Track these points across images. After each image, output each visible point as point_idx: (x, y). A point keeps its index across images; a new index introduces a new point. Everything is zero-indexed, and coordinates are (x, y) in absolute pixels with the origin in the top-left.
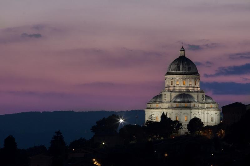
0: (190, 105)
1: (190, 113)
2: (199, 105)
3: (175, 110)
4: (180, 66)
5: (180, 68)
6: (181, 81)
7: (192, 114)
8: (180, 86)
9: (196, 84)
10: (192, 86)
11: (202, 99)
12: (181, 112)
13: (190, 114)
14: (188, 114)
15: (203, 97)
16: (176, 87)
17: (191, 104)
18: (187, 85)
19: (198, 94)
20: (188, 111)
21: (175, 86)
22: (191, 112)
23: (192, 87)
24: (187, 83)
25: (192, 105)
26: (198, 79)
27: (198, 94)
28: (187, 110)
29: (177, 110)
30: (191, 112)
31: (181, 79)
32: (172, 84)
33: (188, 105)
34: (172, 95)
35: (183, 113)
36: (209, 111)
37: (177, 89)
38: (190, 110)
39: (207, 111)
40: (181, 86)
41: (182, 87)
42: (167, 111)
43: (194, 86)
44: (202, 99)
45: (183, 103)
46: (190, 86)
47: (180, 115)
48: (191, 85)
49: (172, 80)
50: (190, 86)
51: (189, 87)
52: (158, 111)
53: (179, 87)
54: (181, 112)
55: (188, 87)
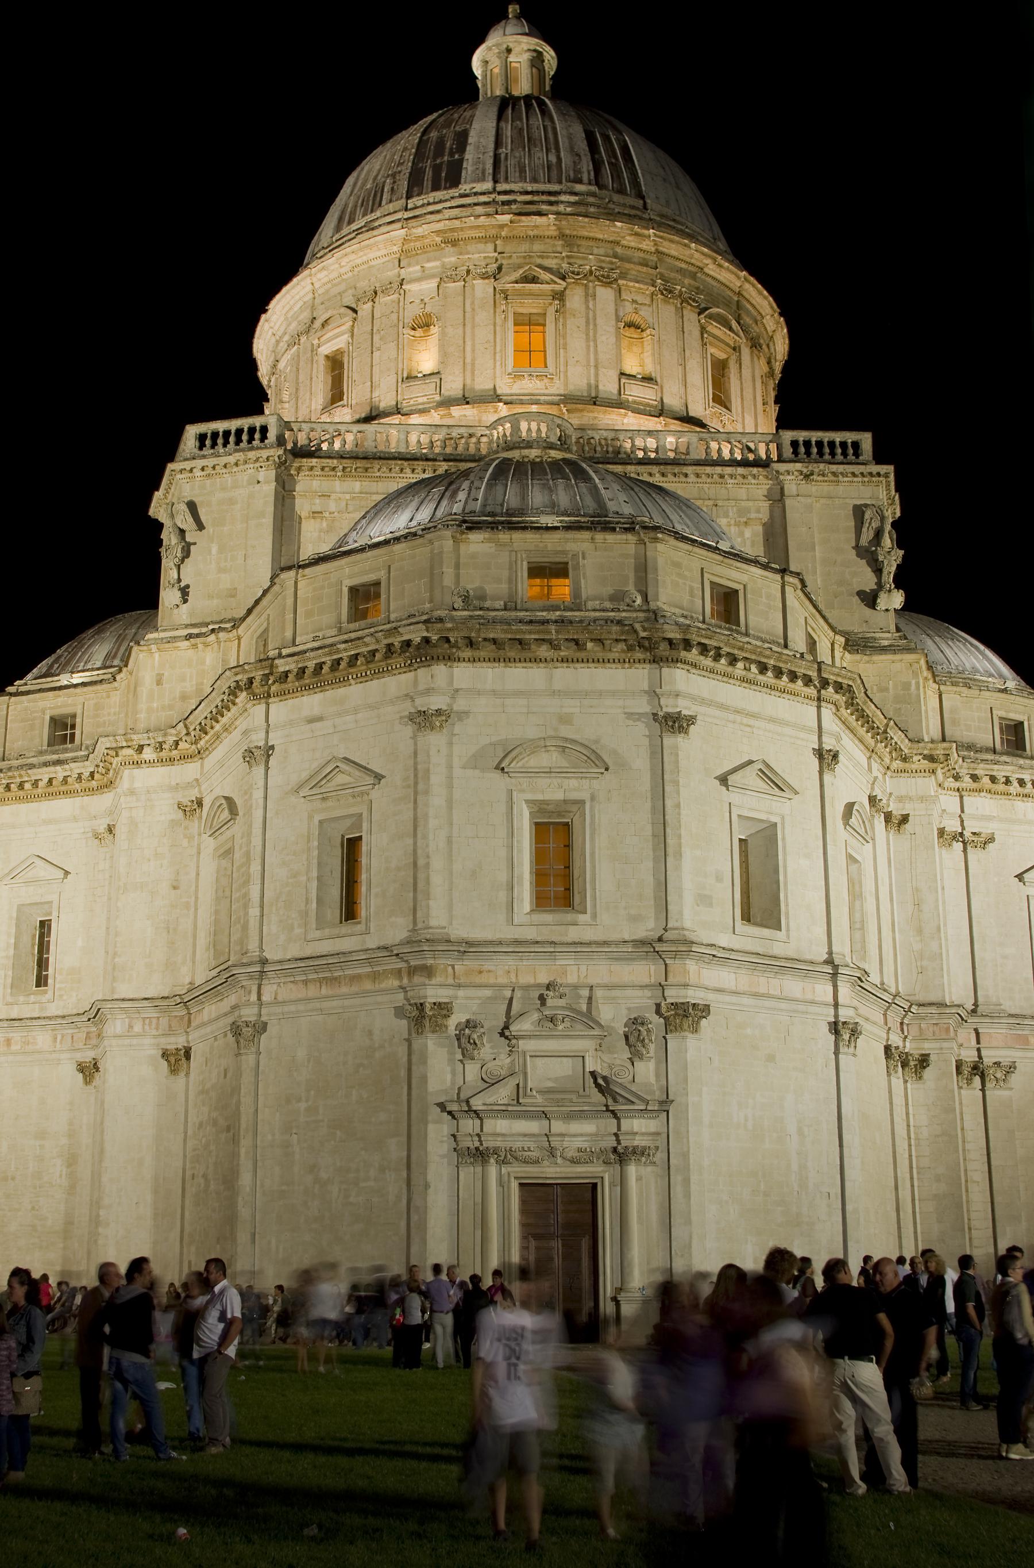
0: (643, 571)
1: (641, 730)
2: (812, 644)
3: (312, 702)
4: (462, 139)
5: (470, 155)
6: (483, 316)
7: (688, 750)
8: (453, 386)
9: (721, 399)
10: (673, 401)
11: (867, 580)
12: (424, 720)
13: (641, 762)
14: (594, 759)
15: (869, 555)
16: (398, 411)
17: (666, 553)
18: (577, 380)
19: (778, 498)
20: (605, 694)
21: (386, 402)
22: (676, 723)
23: (661, 411)
24: (576, 343)
25: (681, 583)
26: (755, 345)
27: (778, 498)
28: (564, 676)
29: (355, 692)
30: (676, 723)
31: (482, 288)
32: (337, 395)
33: (599, 563)
34: (302, 506)
35: (471, 736)
36: (984, 810)
37: (414, 433)
38: (640, 675)
39: (950, 802)
40: (482, 384)
41: (497, 398)
42: (190, 770)
43: (697, 410)
44: (867, 580)
45: (477, 542)
46: (635, 392)
47: (417, 780)
48: (648, 379)
49: (334, 341)
50: (635, 392)
51: (618, 404)
52: (63, 806)
53: (447, 403)
54: (424, 720)
55: (594, 401)
